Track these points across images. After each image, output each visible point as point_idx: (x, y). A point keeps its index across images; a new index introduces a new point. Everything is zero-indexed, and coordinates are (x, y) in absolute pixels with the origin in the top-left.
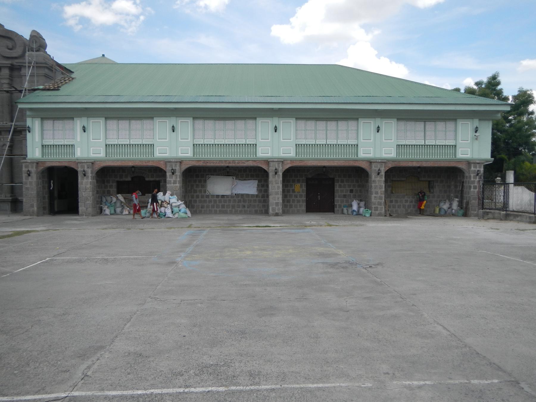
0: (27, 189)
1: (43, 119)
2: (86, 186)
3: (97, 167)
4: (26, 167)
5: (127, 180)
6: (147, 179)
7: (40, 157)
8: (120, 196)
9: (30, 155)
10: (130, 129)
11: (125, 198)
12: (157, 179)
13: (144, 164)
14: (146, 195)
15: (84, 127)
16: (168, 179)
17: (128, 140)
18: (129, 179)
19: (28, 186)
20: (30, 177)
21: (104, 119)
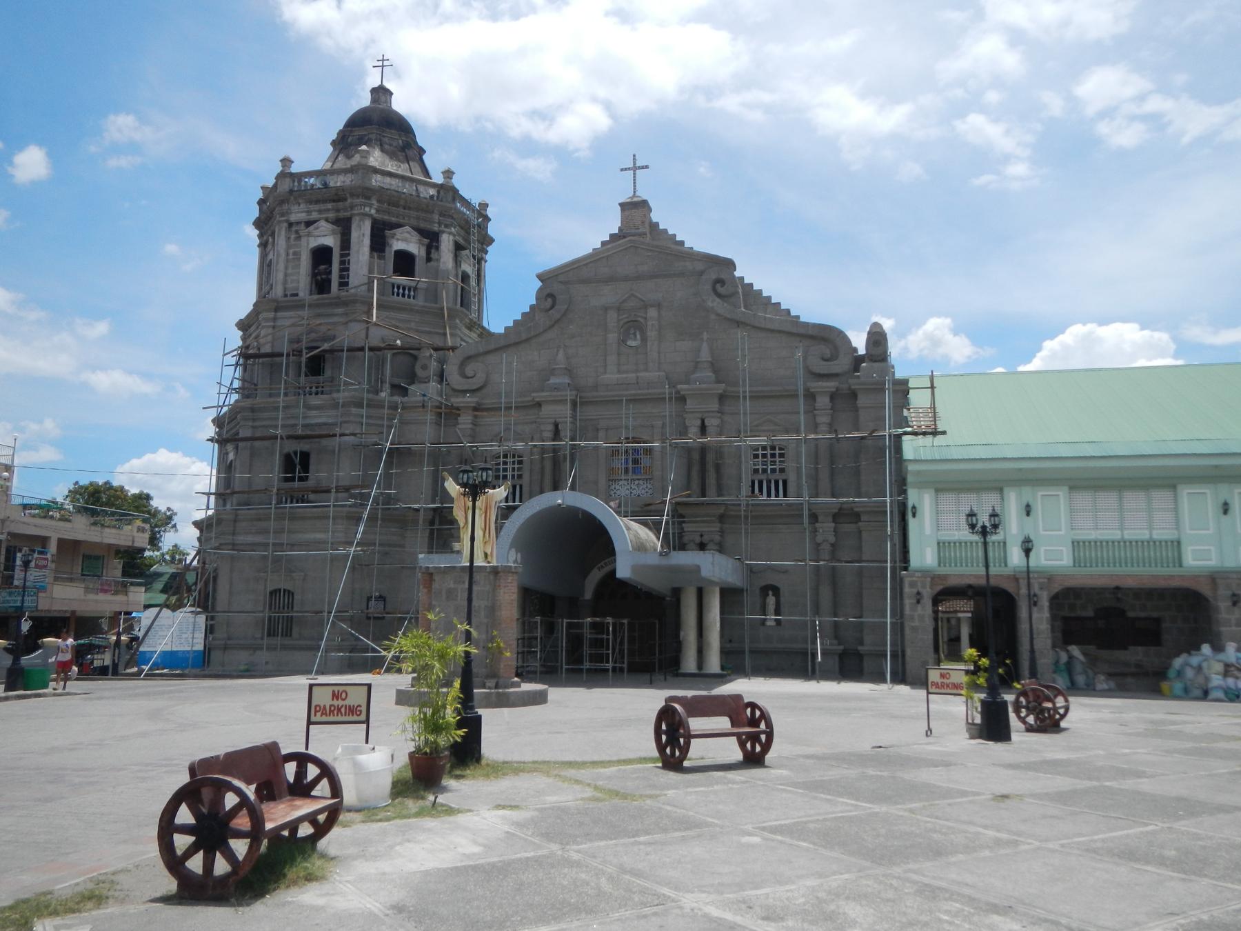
0: (914, 629)
1: (938, 491)
2: (1037, 624)
3: (1056, 588)
4: (912, 585)
5: (1084, 614)
6: (1131, 614)
7: (935, 563)
8: (1075, 650)
9: (915, 561)
10: (1121, 509)
11: (1085, 654)
12: (1155, 615)
13: (1162, 584)
14: (1132, 648)
15: (1028, 506)
16: (1223, 615)
17: (1147, 532)
18: (1090, 613)
19: (916, 623)
20: (919, 607)
21: (1066, 488)
